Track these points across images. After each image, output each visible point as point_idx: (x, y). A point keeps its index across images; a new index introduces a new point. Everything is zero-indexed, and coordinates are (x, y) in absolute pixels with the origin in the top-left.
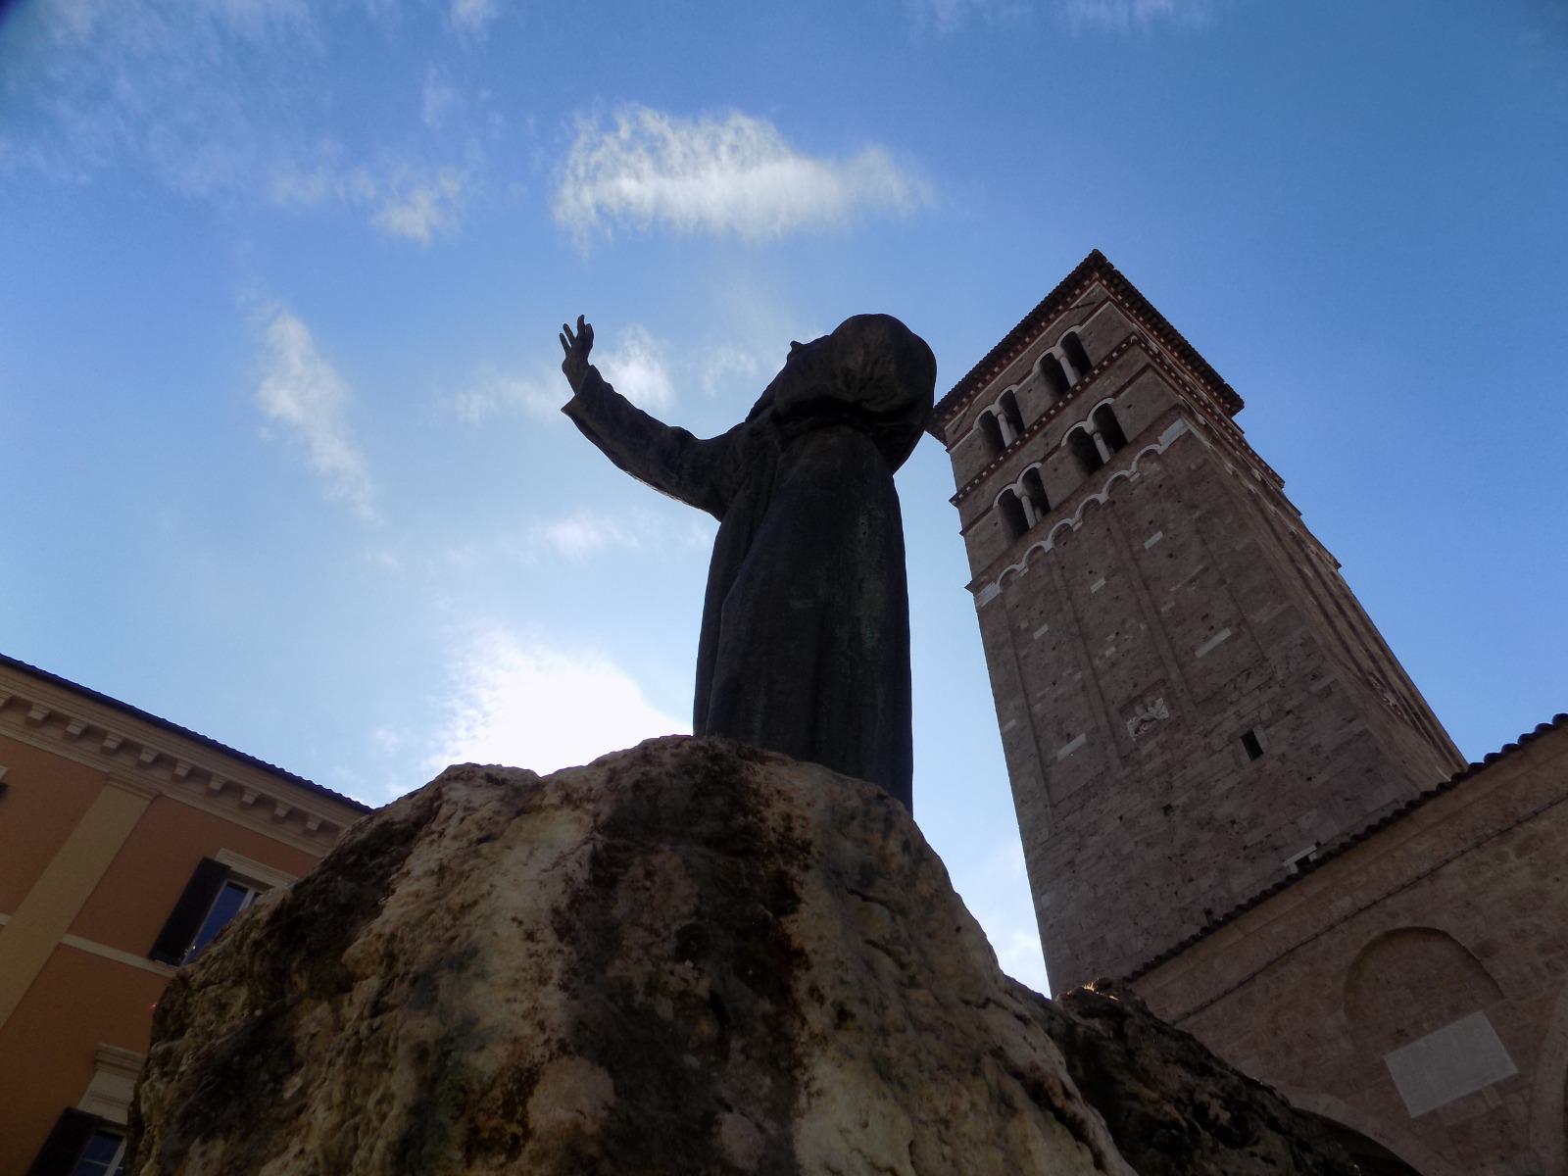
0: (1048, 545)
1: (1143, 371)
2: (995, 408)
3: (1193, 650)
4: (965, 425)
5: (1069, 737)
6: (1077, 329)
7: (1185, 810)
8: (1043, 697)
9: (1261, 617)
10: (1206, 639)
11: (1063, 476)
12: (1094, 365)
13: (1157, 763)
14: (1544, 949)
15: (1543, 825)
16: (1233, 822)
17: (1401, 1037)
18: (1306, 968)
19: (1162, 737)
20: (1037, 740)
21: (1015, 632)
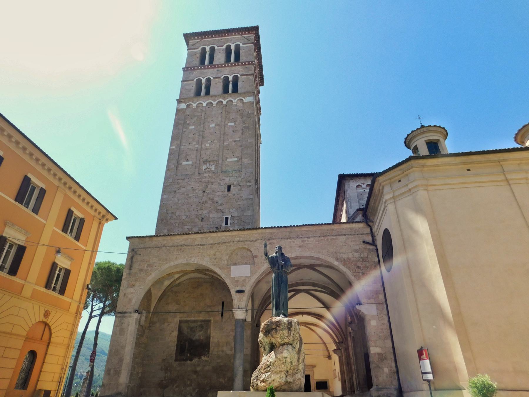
0: (204, 104)
1: (251, 75)
2: (208, 49)
3: (227, 158)
4: (197, 45)
5: (187, 160)
6: (241, 45)
7: (208, 194)
8: (185, 145)
9: (245, 161)
10: (231, 158)
11: (217, 88)
12: (241, 61)
13: (206, 180)
15: (275, 241)
17: (235, 264)
19: (211, 175)
20: (179, 155)
21: (185, 122)
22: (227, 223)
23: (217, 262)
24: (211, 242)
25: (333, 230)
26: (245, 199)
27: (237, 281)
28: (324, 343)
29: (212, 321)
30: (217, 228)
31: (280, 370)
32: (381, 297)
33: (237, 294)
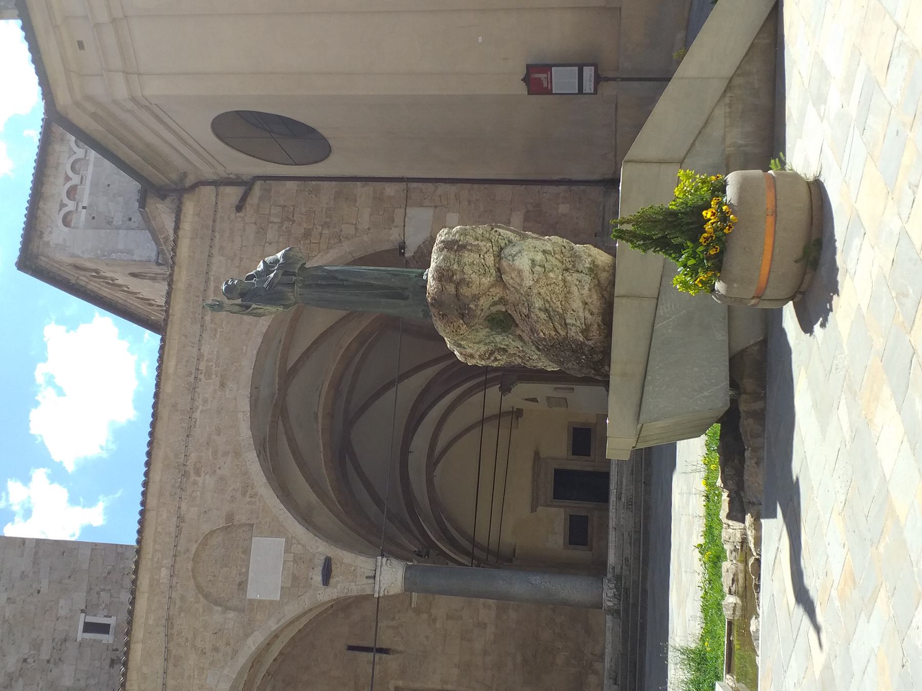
14: (244, 494)
15: (193, 457)
16: (25, 660)
17: (242, 585)
18: (182, 615)
22: (103, 629)
23: (228, 644)
24: (159, 663)
25: (190, 286)
26: (35, 562)
27: (295, 578)
28: (483, 421)
29: (400, 683)
30: (113, 663)
31: (562, 284)
32: (390, 190)
33: (332, 581)
